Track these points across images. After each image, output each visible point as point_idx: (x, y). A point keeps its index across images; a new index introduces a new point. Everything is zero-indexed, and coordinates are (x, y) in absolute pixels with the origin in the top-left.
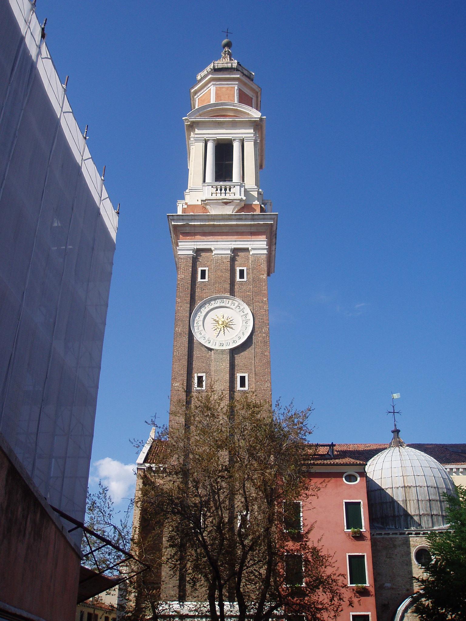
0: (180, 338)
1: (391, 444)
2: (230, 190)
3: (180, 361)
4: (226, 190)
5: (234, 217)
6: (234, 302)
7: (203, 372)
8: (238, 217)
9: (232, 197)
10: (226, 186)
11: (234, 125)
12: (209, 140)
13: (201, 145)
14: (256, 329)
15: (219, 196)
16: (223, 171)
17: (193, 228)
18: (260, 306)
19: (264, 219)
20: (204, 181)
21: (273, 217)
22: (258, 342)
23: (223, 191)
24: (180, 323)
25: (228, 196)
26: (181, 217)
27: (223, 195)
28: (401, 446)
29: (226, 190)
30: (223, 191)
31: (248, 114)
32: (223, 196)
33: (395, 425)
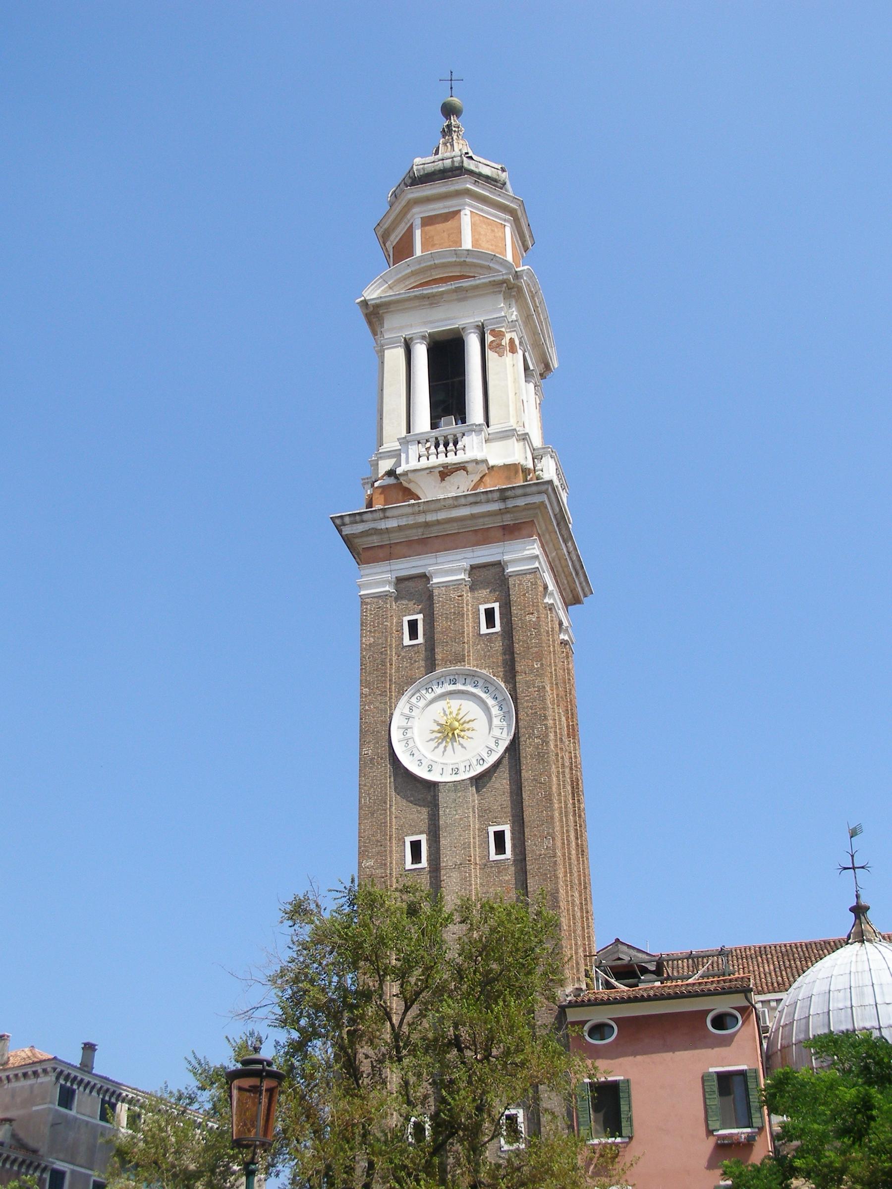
0: (371, 768)
1: (849, 937)
2: (455, 443)
3: (373, 814)
4: (446, 445)
5: (463, 501)
6: (476, 679)
7: (421, 833)
8: (471, 499)
9: (461, 457)
10: (445, 437)
11: (462, 295)
12: (411, 339)
13: (401, 352)
14: (522, 731)
15: (433, 461)
16: (448, 398)
17: (386, 536)
18: (526, 682)
19: (525, 495)
20: (409, 431)
21: (543, 488)
22: (526, 757)
23: (441, 448)
24: (370, 738)
25: (452, 458)
26: (358, 518)
27: (442, 456)
28: (869, 941)
29: (446, 445)
30: (441, 448)
31: (489, 268)
32: (442, 459)
33: (858, 897)
